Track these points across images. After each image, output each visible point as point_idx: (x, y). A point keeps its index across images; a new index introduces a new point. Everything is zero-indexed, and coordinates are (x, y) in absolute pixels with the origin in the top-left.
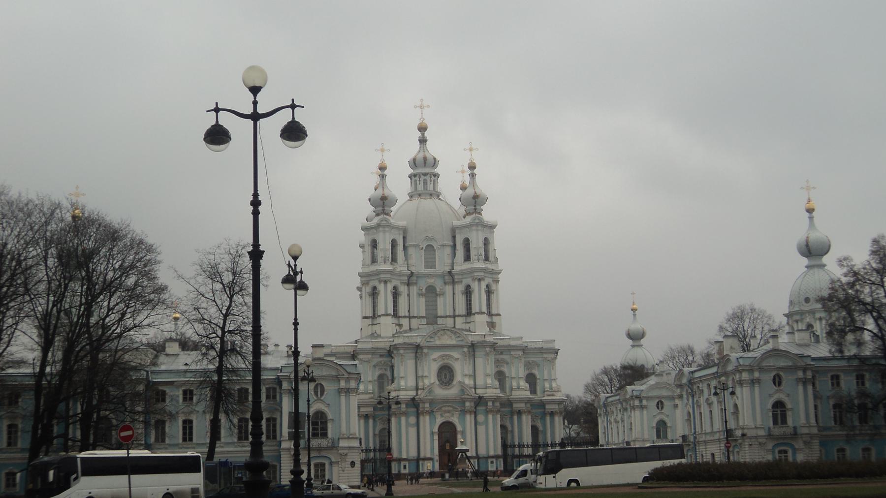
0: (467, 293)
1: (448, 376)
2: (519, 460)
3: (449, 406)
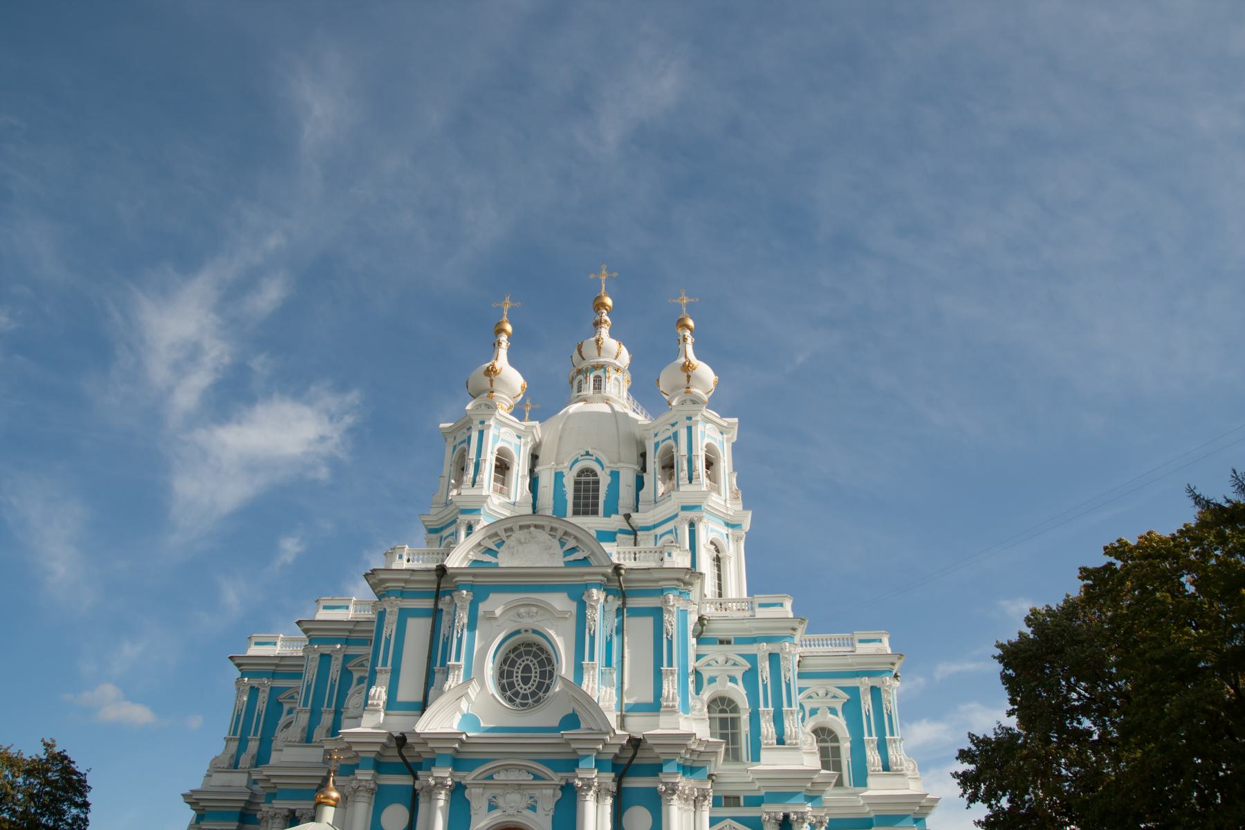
1: (535, 675)
3: (519, 768)
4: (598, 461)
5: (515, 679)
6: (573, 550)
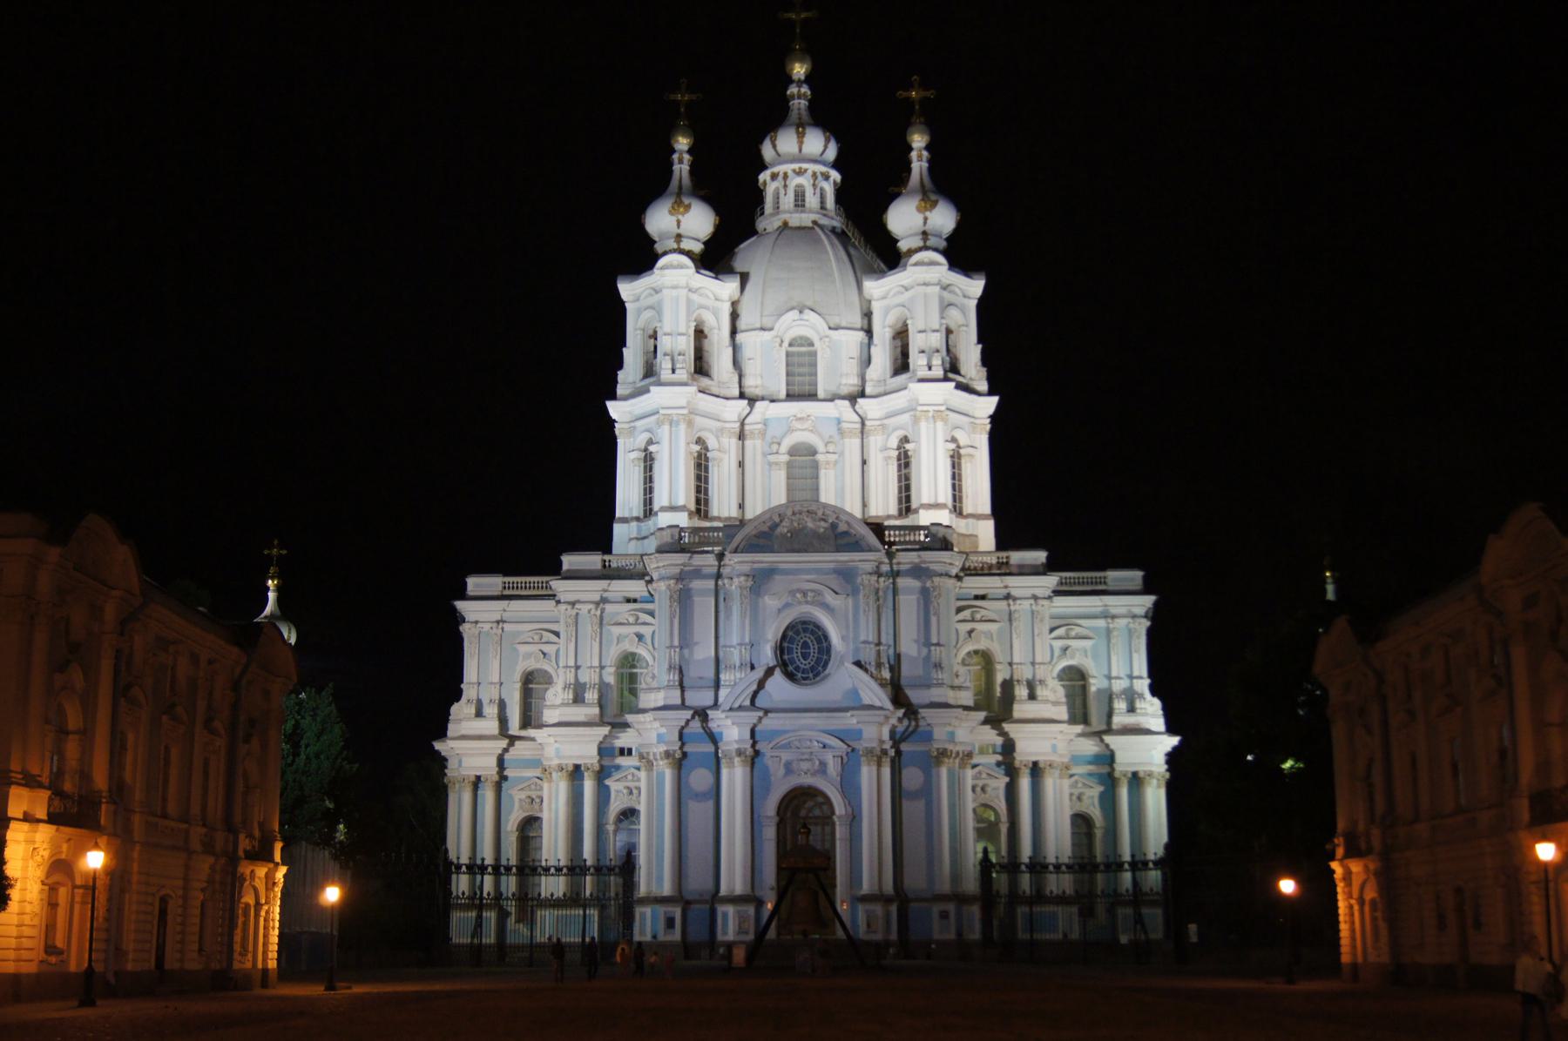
0: (899, 459)
1: (813, 650)
2: (1031, 914)
4: (813, 327)
5: (795, 655)
6: (846, 533)
